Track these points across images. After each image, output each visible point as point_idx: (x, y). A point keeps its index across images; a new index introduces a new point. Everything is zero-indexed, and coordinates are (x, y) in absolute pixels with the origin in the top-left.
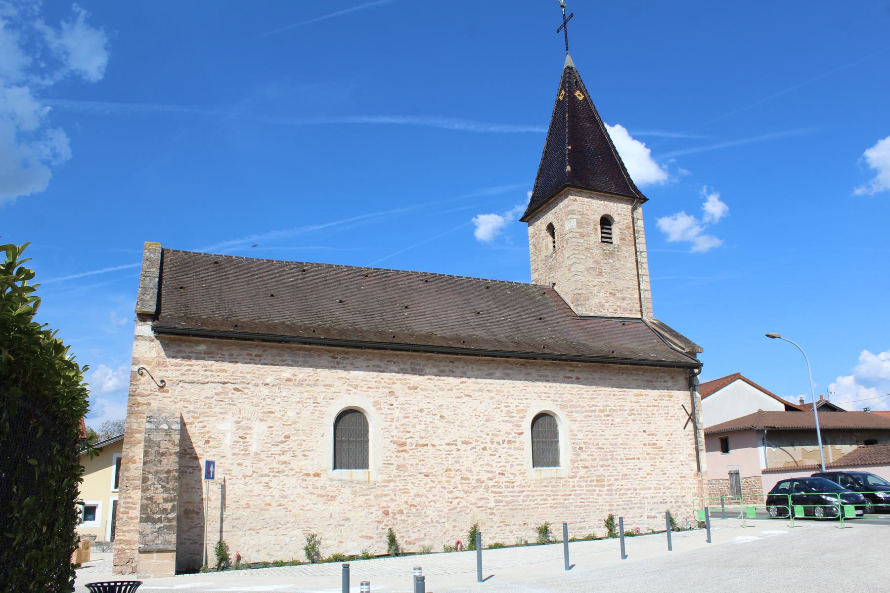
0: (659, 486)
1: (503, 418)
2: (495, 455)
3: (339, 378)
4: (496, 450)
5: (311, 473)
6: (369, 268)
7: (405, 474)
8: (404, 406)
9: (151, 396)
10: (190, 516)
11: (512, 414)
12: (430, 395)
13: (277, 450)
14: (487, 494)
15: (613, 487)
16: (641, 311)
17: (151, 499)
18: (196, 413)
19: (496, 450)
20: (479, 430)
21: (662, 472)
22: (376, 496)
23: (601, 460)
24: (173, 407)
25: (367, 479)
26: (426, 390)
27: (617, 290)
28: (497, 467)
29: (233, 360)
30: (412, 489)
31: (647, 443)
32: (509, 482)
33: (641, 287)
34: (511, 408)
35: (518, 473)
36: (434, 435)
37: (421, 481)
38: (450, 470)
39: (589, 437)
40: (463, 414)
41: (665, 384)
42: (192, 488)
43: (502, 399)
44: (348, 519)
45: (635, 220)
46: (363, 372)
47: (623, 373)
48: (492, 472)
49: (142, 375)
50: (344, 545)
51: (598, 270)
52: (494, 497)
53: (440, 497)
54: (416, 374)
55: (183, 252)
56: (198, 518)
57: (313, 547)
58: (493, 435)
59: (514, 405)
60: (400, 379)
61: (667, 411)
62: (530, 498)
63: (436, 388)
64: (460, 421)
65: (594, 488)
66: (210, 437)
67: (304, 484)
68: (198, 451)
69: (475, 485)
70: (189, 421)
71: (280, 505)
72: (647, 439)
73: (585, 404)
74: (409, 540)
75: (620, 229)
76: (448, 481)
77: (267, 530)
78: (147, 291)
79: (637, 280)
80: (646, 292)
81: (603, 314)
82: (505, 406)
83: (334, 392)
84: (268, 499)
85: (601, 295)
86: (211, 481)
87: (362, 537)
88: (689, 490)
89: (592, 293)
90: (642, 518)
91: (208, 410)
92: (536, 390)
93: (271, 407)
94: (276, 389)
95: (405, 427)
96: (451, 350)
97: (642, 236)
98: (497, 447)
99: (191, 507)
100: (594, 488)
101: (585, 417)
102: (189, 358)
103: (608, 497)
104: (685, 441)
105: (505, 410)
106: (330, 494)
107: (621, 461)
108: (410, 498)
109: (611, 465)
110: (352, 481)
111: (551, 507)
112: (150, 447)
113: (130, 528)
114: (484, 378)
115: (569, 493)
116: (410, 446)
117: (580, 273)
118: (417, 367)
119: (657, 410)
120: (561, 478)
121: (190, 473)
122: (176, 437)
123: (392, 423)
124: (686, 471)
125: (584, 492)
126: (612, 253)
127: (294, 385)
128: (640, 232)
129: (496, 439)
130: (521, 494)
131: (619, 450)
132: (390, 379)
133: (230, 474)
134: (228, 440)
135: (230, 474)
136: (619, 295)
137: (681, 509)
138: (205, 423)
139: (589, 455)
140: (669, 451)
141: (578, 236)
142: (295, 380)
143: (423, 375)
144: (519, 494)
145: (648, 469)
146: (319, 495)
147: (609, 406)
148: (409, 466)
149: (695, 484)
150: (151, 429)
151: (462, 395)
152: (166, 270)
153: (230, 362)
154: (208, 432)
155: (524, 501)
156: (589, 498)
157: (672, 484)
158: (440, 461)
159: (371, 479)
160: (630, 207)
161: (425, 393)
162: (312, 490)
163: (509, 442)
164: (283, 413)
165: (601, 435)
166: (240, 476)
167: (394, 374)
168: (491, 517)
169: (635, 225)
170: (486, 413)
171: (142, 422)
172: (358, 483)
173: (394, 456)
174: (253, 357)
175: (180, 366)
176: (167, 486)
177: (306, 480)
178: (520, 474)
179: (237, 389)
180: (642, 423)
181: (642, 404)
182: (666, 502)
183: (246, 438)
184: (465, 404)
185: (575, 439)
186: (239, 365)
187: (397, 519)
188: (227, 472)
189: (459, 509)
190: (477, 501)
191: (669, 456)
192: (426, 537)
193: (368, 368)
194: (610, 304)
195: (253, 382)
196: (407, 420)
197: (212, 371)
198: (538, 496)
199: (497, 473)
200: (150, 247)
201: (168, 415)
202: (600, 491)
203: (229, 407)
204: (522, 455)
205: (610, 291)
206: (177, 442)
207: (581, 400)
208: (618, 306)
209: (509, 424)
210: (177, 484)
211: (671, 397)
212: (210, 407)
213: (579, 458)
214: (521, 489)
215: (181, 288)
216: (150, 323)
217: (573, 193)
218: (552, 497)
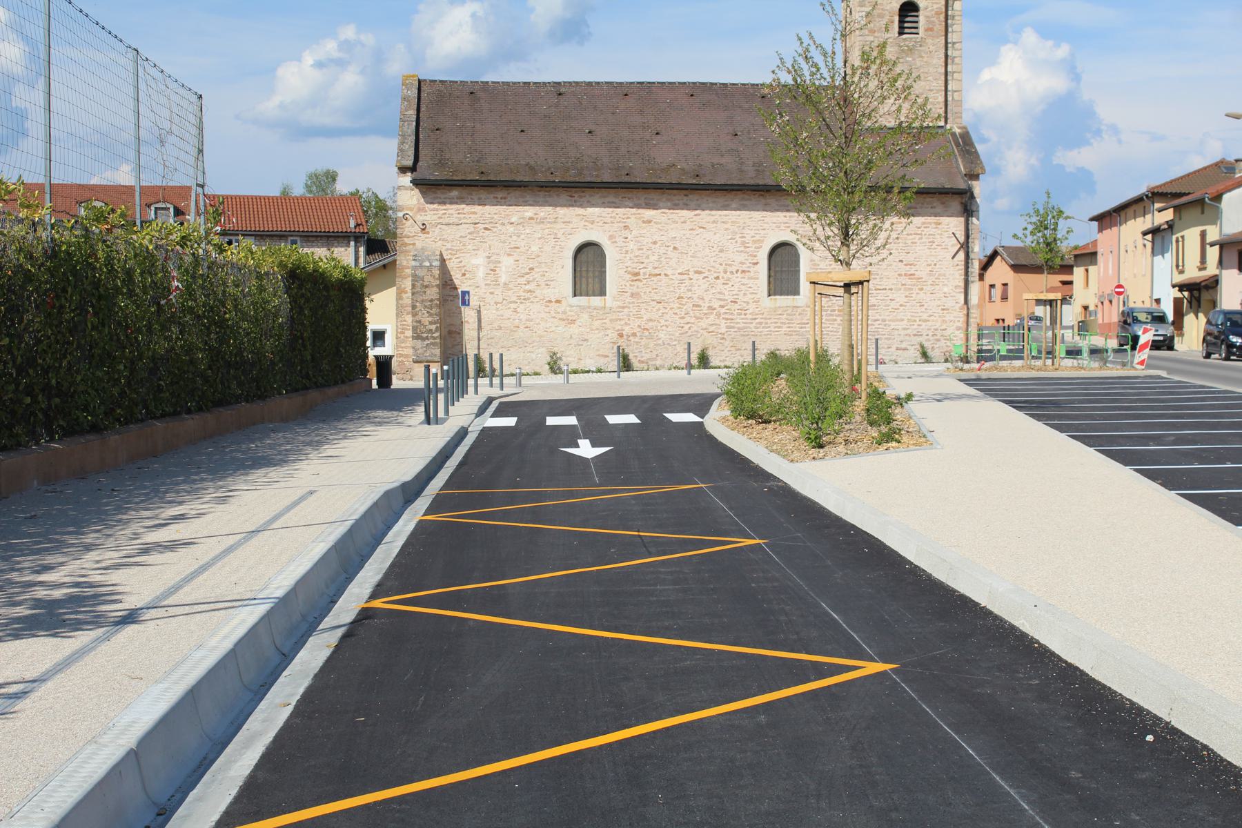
2: (727, 284)
3: (576, 215)
4: (729, 279)
5: (554, 300)
6: (631, 83)
8: (637, 239)
9: (416, 238)
10: (453, 335)
11: (747, 245)
13: (523, 280)
17: (420, 322)
18: (453, 250)
19: (729, 279)
21: (918, 304)
24: (434, 246)
25: (603, 305)
28: (729, 295)
29: (482, 203)
31: (903, 273)
32: (741, 310)
33: (950, 88)
34: (747, 238)
35: (751, 301)
38: (682, 298)
39: (832, 267)
41: (932, 210)
42: (453, 313)
43: (737, 230)
44: (586, 340)
46: (599, 209)
48: (724, 300)
50: (582, 362)
52: (726, 323)
53: (672, 322)
54: (650, 209)
55: (441, 81)
56: (460, 338)
57: (555, 363)
60: (634, 214)
61: (931, 240)
62: (763, 325)
65: (835, 317)
66: (465, 271)
67: (547, 310)
68: (457, 282)
70: (449, 256)
71: (527, 327)
72: (904, 269)
74: (642, 359)
75: (927, 17)
76: (680, 308)
77: (517, 348)
78: (406, 139)
79: (944, 79)
80: (955, 94)
82: (740, 237)
86: (467, 308)
87: (599, 355)
90: (890, 350)
91: (463, 247)
92: (774, 220)
93: (517, 243)
94: (521, 227)
96: (680, 187)
97: (958, 22)
99: (453, 329)
102: (444, 203)
105: (739, 240)
106: (571, 318)
110: (589, 307)
111: (785, 334)
112: (417, 281)
113: (407, 345)
114: (719, 210)
115: (807, 322)
118: (651, 202)
119: (919, 239)
121: (451, 301)
122: (436, 272)
123: (627, 255)
124: (950, 303)
126: (911, 50)
127: (536, 223)
128: (956, 18)
129: (729, 269)
132: (624, 214)
133: (484, 301)
134: (481, 273)
135: (484, 301)
137: (938, 343)
138: (462, 259)
140: (930, 282)
142: (537, 218)
143: (657, 209)
145: (902, 300)
146: (560, 319)
148: (642, 294)
150: (416, 266)
152: (422, 109)
153: (479, 205)
154: (464, 266)
156: (829, 327)
158: (672, 289)
159: (607, 305)
161: (659, 226)
162: (554, 315)
163: (743, 271)
164: (527, 248)
166: (492, 303)
167: (628, 209)
168: (722, 341)
169: (950, 8)
170: (720, 244)
171: (410, 259)
172: (595, 309)
174: (499, 200)
175: (437, 211)
177: (548, 306)
179: (486, 229)
180: (899, 253)
182: (921, 335)
183: (495, 271)
185: (817, 269)
186: (487, 207)
187: (630, 341)
188: (481, 299)
189: (689, 334)
191: (929, 288)
192: (659, 358)
193: (604, 205)
195: (501, 221)
196: (641, 252)
197: (464, 214)
200: (407, 82)
201: (430, 253)
204: (756, 284)
206: (437, 276)
209: (743, 255)
210: (438, 310)
211: (940, 224)
212: (464, 245)
214: (754, 317)
215: (437, 130)
216: (409, 174)
218: (788, 325)
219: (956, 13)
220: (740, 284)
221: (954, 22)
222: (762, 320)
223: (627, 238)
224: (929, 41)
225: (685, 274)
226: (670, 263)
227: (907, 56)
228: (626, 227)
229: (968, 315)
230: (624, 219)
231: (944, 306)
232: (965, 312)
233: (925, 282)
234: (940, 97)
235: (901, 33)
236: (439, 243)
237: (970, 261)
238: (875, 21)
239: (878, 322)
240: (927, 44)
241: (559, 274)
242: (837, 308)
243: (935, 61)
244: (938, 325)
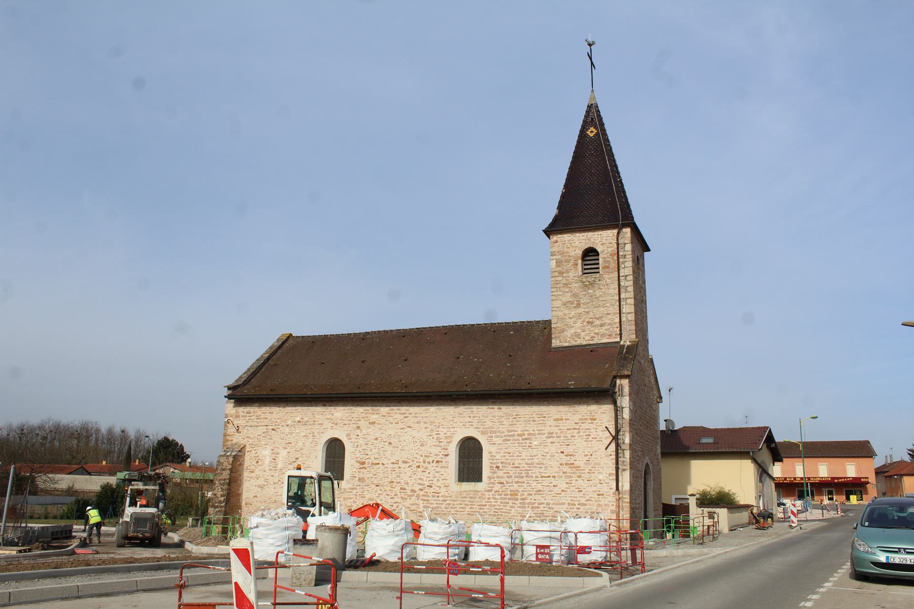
0: (573, 502)
2: (425, 472)
3: (327, 419)
10: (248, 506)
11: (441, 440)
12: (383, 428)
15: (526, 501)
16: (621, 334)
17: (215, 495)
22: (344, 499)
23: (516, 477)
26: (381, 424)
30: (367, 494)
32: (435, 493)
33: (624, 311)
34: (441, 435)
35: (442, 486)
36: (384, 457)
37: (373, 489)
38: (393, 482)
39: (506, 458)
40: (405, 441)
43: (433, 428)
47: (544, 401)
48: (423, 485)
51: (575, 302)
52: (423, 503)
58: (425, 456)
59: (443, 433)
60: (364, 418)
61: (588, 433)
62: (451, 506)
63: (388, 422)
64: (402, 446)
65: (507, 501)
66: (259, 459)
69: (409, 494)
72: (565, 459)
73: (504, 430)
75: (605, 258)
76: (391, 490)
82: (436, 434)
83: (324, 429)
85: (579, 324)
88: (606, 507)
89: (567, 325)
94: (292, 428)
95: (365, 451)
97: (628, 260)
100: (507, 501)
101: (504, 440)
103: (520, 510)
104: (606, 462)
105: (435, 436)
107: (537, 479)
108: (365, 501)
109: (526, 482)
111: (468, 514)
112: (219, 466)
115: (484, 504)
116: (368, 464)
117: (556, 309)
119: (579, 433)
120: (479, 491)
122: (231, 459)
124: (604, 489)
125: (499, 503)
128: (627, 257)
129: (427, 460)
130: (444, 503)
131: (534, 469)
134: (267, 460)
136: (598, 322)
139: (505, 473)
141: (557, 274)
147: (528, 431)
149: (614, 502)
151: (405, 426)
154: (258, 456)
155: (447, 508)
156: (502, 509)
157: (587, 500)
158: (387, 475)
163: (438, 462)
165: (517, 456)
166: (272, 483)
170: (421, 440)
178: (444, 487)
179: (273, 429)
180: (560, 445)
183: (275, 459)
184: (406, 434)
185: (493, 460)
188: (266, 480)
190: (411, 506)
191: (586, 476)
195: (281, 424)
196: (367, 446)
198: (458, 504)
202: (513, 503)
203: (270, 440)
204: (447, 472)
206: (231, 462)
207: (500, 426)
208: (595, 333)
210: (227, 487)
211: (595, 419)
213: (495, 475)
214: (444, 499)
220: (434, 471)
221: (625, 260)
222: (451, 502)
223: (358, 436)
224: (606, 276)
225: (396, 463)
226: (386, 455)
227: (589, 289)
228: (358, 428)
230: (356, 421)
231: (600, 491)
233: (583, 470)
238: (563, 265)
239: (543, 505)
241: (314, 463)
242: (509, 493)
244: (594, 509)
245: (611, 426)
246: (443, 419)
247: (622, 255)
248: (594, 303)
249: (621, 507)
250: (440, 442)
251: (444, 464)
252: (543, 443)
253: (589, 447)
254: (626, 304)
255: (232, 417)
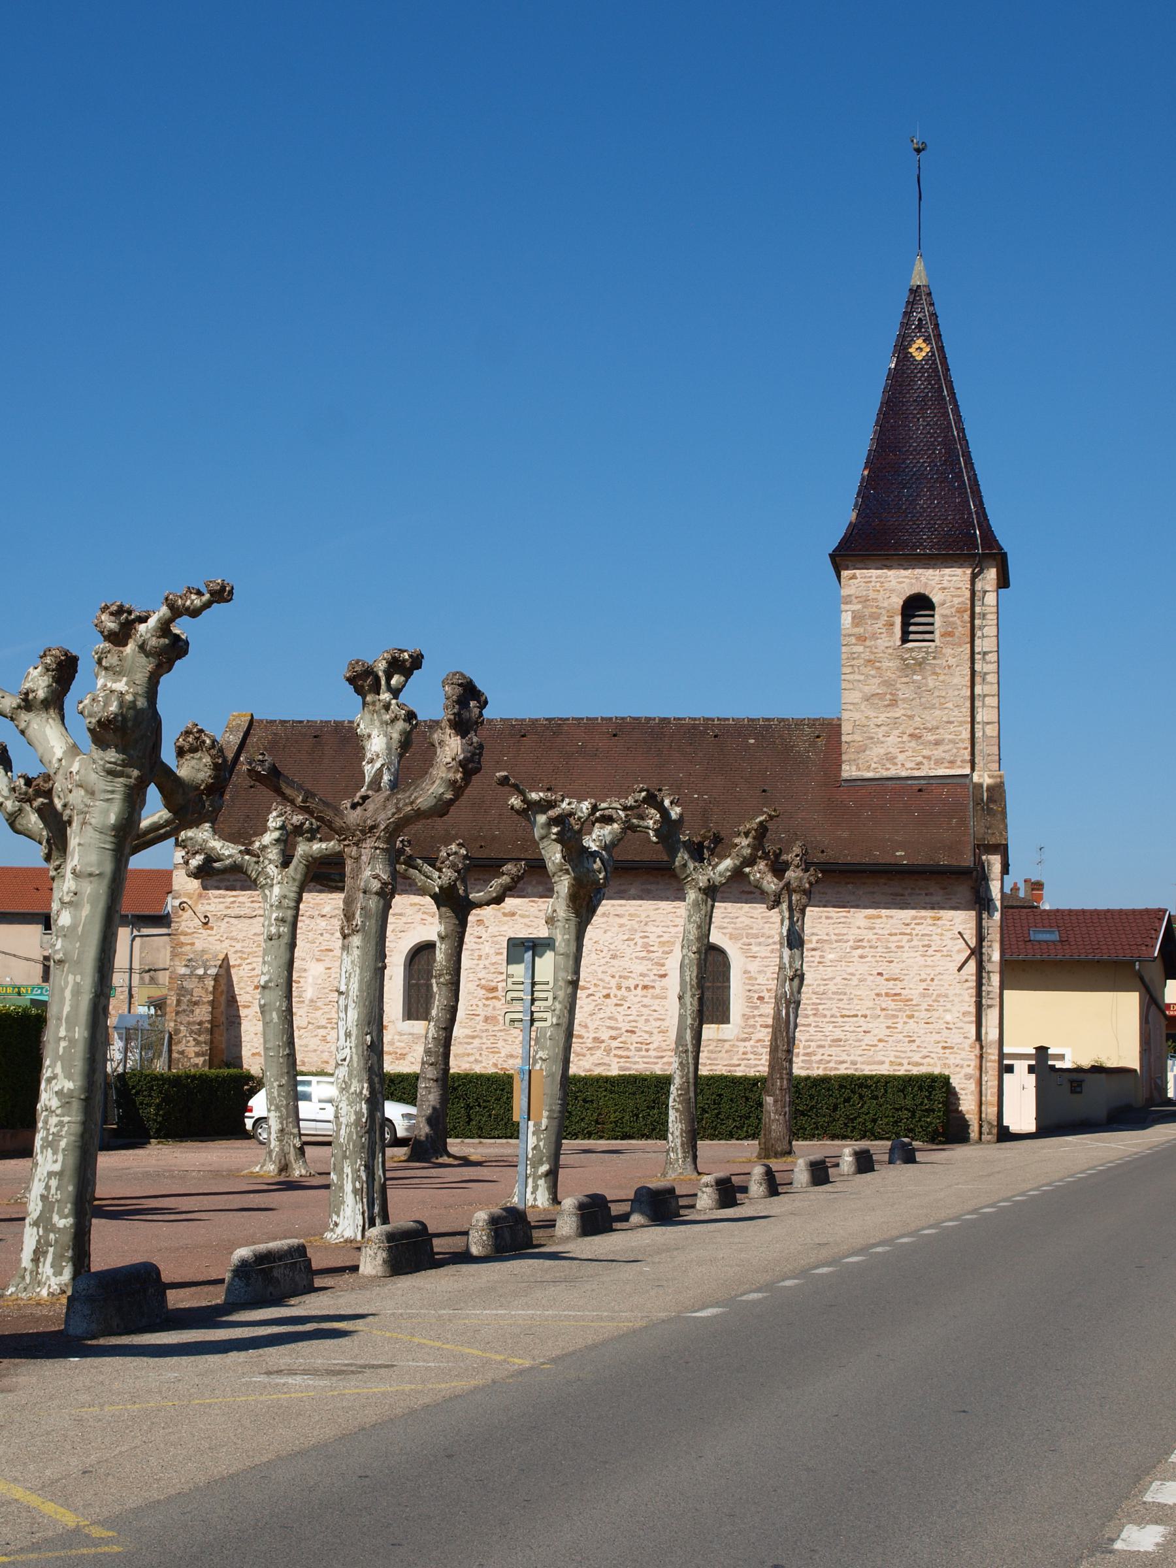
1: (638, 954)
2: (622, 1005)
3: (411, 905)
4: (624, 999)
7: (495, 1029)
8: (495, 939)
9: (195, 935)
11: (652, 949)
14: (608, 1058)
15: (813, 1058)
19: (624, 999)
20: (601, 969)
24: (218, 948)
27: (924, 728)
31: (883, 992)
32: (641, 1043)
33: (978, 718)
34: (651, 939)
35: (655, 1031)
41: (928, 899)
43: (636, 926)
45: (978, 595)
49: (183, 910)
51: (888, 697)
58: (620, 977)
61: (927, 943)
69: (590, 1046)
70: (239, 962)
72: (884, 986)
75: (943, 616)
80: (988, 726)
81: (892, 772)
84: (325, 1056)
85: (893, 740)
88: (958, 1069)
89: (872, 738)
98: (626, 994)
106: (399, 1051)
107: (833, 1019)
109: (813, 1024)
112: (183, 996)
115: (737, 1062)
117: (851, 707)
119: (908, 941)
120: (725, 1041)
122: (210, 983)
124: (955, 1038)
126: (921, 664)
128: (989, 616)
129: (625, 983)
130: (659, 1060)
136: (930, 737)
140: (924, 1006)
141: (853, 640)
144: (655, 1060)
145: (882, 1032)
149: (971, 1060)
150: (185, 975)
160: (969, 571)
161: (526, 920)
163: (645, 987)
169: (977, 603)
170: (612, 947)
173: (480, 1003)
176: (199, 1039)
181: (880, 932)
185: (753, 985)
191: (924, 1014)
194: (910, 753)
199: (624, 1030)
204: (663, 1006)
205: (910, 731)
206: (211, 989)
208: (924, 757)
213: (756, 1012)
217: (850, 564)
219: (989, 610)
220: (640, 1005)
224: (948, 651)
229: (981, 1057)
232: (977, 1052)
234: (964, 732)
235: (905, 640)
236: (227, 943)
237: (984, 975)
238: (867, 624)
239: (845, 1065)
240: (944, 655)
243: (955, 681)
245: (968, 931)
246: (657, 909)
247: (979, 613)
248: (923, 700)
249: (984, 1069)
250: (649, 952)
251: (657, 991)
252: (845, 957)
253: (928, 966)
254: (984, 706)
255: (191, 898)
